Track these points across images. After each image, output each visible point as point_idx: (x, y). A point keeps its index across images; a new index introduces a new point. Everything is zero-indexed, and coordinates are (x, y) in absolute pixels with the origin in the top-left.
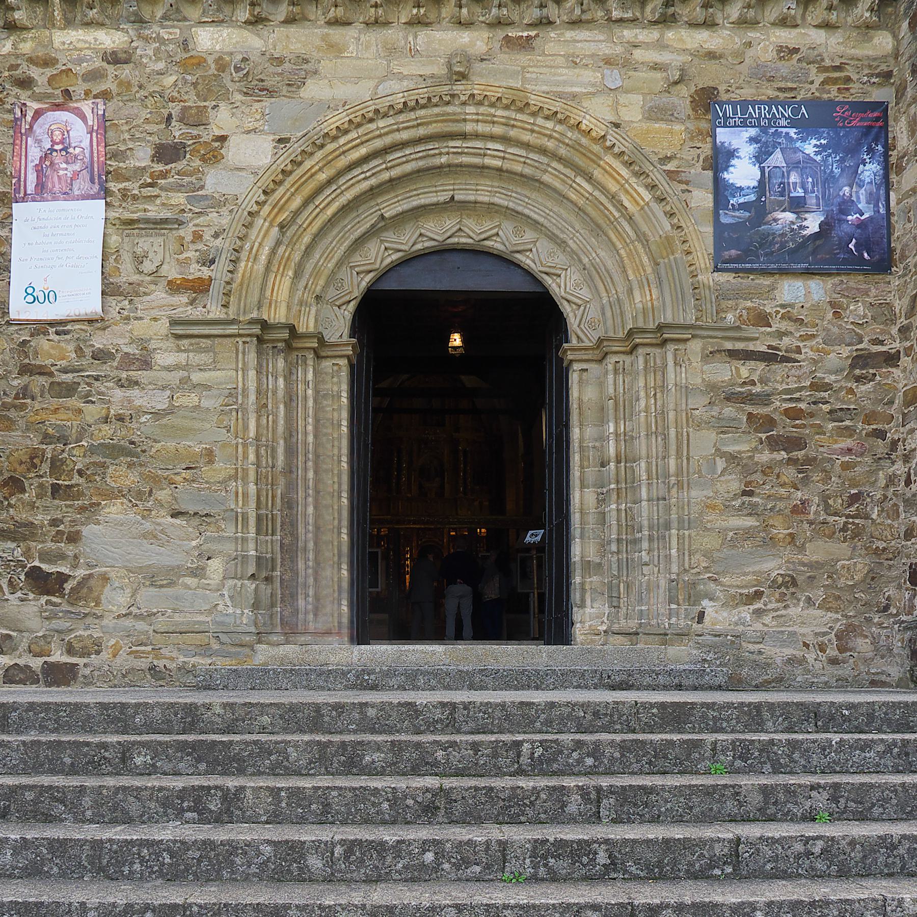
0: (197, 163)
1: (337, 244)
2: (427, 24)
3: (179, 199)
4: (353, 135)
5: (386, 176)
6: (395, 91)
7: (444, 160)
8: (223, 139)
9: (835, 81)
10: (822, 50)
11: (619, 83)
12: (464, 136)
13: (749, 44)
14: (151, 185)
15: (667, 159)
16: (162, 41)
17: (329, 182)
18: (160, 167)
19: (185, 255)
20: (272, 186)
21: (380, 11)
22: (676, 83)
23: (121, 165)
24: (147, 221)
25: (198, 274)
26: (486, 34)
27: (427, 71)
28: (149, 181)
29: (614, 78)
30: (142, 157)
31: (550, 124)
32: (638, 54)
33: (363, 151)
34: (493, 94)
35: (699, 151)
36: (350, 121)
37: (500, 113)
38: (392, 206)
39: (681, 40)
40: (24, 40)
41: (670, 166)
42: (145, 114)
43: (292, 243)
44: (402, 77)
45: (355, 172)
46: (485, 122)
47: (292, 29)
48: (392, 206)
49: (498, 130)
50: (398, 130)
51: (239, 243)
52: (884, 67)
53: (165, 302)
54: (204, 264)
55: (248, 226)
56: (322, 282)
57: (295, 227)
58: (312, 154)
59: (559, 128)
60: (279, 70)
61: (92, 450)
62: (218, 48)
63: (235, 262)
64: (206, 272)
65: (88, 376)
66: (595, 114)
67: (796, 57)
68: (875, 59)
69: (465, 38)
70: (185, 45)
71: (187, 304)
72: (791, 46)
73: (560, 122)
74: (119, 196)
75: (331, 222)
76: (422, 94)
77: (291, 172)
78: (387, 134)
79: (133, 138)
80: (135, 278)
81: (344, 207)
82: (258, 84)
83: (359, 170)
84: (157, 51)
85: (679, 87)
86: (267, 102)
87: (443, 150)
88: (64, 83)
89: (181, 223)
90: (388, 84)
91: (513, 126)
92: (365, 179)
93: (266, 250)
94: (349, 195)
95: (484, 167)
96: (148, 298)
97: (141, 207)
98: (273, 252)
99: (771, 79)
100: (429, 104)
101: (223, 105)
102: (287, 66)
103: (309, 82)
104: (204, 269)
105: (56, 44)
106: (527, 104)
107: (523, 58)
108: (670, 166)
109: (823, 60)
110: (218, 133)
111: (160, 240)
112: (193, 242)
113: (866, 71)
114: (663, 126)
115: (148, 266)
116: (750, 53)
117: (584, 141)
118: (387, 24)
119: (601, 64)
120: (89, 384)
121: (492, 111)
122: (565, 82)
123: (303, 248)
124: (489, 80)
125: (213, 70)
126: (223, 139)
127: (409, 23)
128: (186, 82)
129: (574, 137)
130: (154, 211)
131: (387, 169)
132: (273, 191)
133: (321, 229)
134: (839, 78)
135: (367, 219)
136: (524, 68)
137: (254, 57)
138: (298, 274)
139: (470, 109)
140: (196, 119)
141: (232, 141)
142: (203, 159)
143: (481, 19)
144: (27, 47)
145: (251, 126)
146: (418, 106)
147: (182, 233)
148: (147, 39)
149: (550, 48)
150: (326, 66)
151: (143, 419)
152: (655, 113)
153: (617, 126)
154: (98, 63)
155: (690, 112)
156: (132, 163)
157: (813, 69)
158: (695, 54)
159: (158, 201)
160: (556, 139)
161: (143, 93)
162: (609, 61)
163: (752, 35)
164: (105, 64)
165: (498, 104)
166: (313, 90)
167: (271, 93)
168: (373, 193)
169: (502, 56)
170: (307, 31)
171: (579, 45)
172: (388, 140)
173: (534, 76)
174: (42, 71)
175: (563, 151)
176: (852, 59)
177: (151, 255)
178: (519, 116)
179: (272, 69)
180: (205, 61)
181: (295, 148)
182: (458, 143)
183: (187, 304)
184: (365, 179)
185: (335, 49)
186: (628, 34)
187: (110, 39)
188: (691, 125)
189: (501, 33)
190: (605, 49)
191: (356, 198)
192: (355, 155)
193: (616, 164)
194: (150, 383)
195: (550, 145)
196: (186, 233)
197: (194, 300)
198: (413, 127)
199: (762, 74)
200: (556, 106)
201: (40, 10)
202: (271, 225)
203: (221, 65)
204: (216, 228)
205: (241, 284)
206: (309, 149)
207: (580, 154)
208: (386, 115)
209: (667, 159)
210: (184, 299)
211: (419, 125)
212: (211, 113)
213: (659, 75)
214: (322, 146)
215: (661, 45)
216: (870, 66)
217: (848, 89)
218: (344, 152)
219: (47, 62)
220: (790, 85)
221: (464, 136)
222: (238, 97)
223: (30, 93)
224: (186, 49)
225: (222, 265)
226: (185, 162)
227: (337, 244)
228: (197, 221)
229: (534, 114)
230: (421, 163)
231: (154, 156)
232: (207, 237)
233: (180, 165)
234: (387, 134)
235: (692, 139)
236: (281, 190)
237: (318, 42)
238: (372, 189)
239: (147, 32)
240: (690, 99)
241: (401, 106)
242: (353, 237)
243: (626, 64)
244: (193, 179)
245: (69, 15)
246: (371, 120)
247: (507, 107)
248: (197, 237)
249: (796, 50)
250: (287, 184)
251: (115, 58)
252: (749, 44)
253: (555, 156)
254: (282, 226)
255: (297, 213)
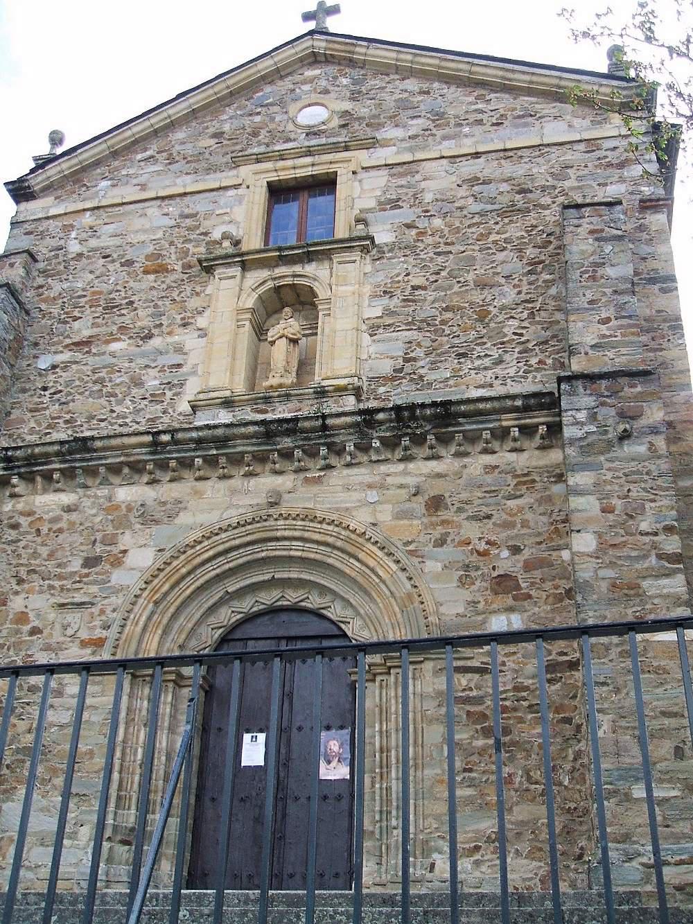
0: (108, 567)
1: (195, 611)
2: (256, 475)
3: (94, 589)
4: (206, 543)
5: (227, 567)
6: (233, 515)
7: (263, 554)
8: (125, 552)
9: (525, 483)
10: (514, 465)
11: (376, 499)
12: (277, 539)
13: (465, 466)
14: (79, 582)
15: (408, 543)
16: (96, 496)
17: (189, 573)
18: (86, 571)
19: (94, 624)
20: (150, 578)
21: (226, 470)
22: (414, 495)
23: (63, 571)
24: (73, 604)
25: (100, 636)
26: (292, 476)
27: (254, 502)
28: (78, 579)
29: (373, 496)
30: (76, 565)
31: (330, 528)
32: (389, 480)
33: (211, 553)
34: (294, 513)
35: (429, 536)
36: (203, 536)
37: (300, 523)
38: (233, 586)
39: (419, 468)
40: (19, 503)
41: (411, 547)
42: (81, 540)
43: (163, 613)
44: (238, 507)
45: (207, 566)
46: (290, 529)
47: (174, 485)
48: (233, 586)
49: (297, 534)
50: (234, 539)
51: (126, 614)
52: (558, 471)
53: (77, 654)
54: (104, 629)
55: (133, 604)
56: (183, 636)
57: (165, 603)
58: (178, 557)
59: (336, 529)
60: (163, 509)
61: (18, 751)
62: (129, 499)
63: (123, 626)
64: (105, 633)
65: (23, 703)
66: (360, 519)
67: (497, 471)
68: (552, 467)
69: (279, 480)
70: (110, 499)
71: (90, 655)
72: (493, 464)
73: (337, 526)
74: (59, 589)
75: (190, 598)
76: (249, 517)
77: (163, 569)
78: (227, 541)
79: (72, 555)
80: (62, 639)
81: (198, 588)
82: (148, 518)
83: (210, 564)
84: (94, 503)
85: (416, 497)
86: (154, 528)
87: (264, 549)
88: (38, 525)
89: (93, 604)
90: (229, 512)
91: (308, 531)
92: (214, 569)
93: (144, 618)
94: (201, 581)
95: (291, 557)
96: (66, 651)
97: (71, 595)
98: (149, 618)
99: (480, 486)
100: (253, 521)
101: (128, 532)
102: (169, 506)
103: (181, 514)
104: (104, 631)
105: (37, 503)
106: (316, 517)
107: (315, 489)
108: (411, 547)
109: (515, 471)
110: (123, 548)
111: (79, 615)
112: (99, 615)
113: (546, 475)
114: (406, 522)
115: (70, 632)
116: (466, 471)
117: (353, 536)
118: (230, 477)
119: (365, 488)
120: (23, 708)
121: (294, 522)
122: (341, 501)
123: (170, 615)
124: (294, 504)
125: (124, 511)
126: (125, 552)
127: (245, 475)
128: (107, 519)
129: (346, 534)
130: (78, 598)
131: (228, 562)
132: (152, 581)
133: (183, 603)
134: (528, 481)
135: (216, 594)
136: (315, 495)
137: (149, 502)
138: (165, 632)
139: (281, 522)
140: (110, 541)
141: (129, 554)
142: (112, 564)
143: (290, 468)
144: (20, 506)
145: (143, 543)
146: (247, 523)
147: (93, 610)
148: (89, 497)
149: (333, 481)
150: (192, 504)
151: (52, 730)
152: (399, 516)
153: (374, 525)
154: (59, 512)
155: (425, 512)
156: (69, 569)
157: (509, 477)
158: (429, 476)
159: (82, 591)
160: (334, 536)
161: (82, 528)
162: (370, 486)
163: (466, 460)
164: (62, 513)
165: (298, 518)
166: (184, 519)
167: (157, 522)
168: (219, 578)
169: (302, 489)
170: (182, 485)
171: (351, 478)
172: (227, 545)
173: (321, 499)
174: (26, 518)
175: (339, 543)
176: (536, 468)
177: (72, 625)
178: (311, 524)
179: (159, 509)
180: (120, 507)
181: (168, 554)
182: (273, 544)
183: (90, 655)
184: (214, 569)
185: (198, 494)
186: (383, 468)
187: (66, 498)
188: (425, 520)
189: (302, 476)
190: (368, 479)
191: (207, 582)
192: (206, 556)
193: (374, 549)
194: (61, 706)
195: (330, 540)
196: (95, 610)
197: (96, 651)
198: (244, 536)
199: (475, 485)
200: (334, 517)
201: (30, 486)
202: (149, 602)
203: (129, 509)
204: (114, 606)
205: (126, 640)
206: (175, 555)
207: (352, 543)
208: (226, 531)
209: (408, 543)
210: (89, 651)
211: (247, 535)
212: (120, 537)
213: (403, 491)
214: (185, 552)
215: (405, 473)
216: (548, 472)
217: (533, 487)
218: (199, 555)
219: (30, 514)
220: (493, 488)
221: (277, 539)
222: (139, 526)
223: (17, 531)
224: (110, 501)
225: (115, 629)
226: (101, 567)
227: (195, 611)
228: (103, 603)
229: (320, 522)
230: (249, 558)
231: (83, 564)
232: (108, 612)
233: (98, 569)
234: (227, 541)
235: (426, 529)
236: (156, 581)
237: (189, 491)
238: (218, 575)
239: (89, 493)
240: (425, 504)
241: (236, 524)
242: (206, 606)
243: (382, 487)
244: (104, 577)
245: (46, 487)
246: (217, 534)
247: (303, 520)
248: (102, 612)
249: (497, 467)
250: (161, 577)
251: (69, 509)
252: (465, 466)
253: (334, 547)
254: (156, 603)
255: (166, 594)
